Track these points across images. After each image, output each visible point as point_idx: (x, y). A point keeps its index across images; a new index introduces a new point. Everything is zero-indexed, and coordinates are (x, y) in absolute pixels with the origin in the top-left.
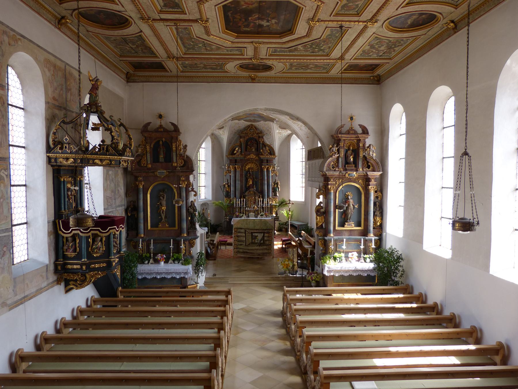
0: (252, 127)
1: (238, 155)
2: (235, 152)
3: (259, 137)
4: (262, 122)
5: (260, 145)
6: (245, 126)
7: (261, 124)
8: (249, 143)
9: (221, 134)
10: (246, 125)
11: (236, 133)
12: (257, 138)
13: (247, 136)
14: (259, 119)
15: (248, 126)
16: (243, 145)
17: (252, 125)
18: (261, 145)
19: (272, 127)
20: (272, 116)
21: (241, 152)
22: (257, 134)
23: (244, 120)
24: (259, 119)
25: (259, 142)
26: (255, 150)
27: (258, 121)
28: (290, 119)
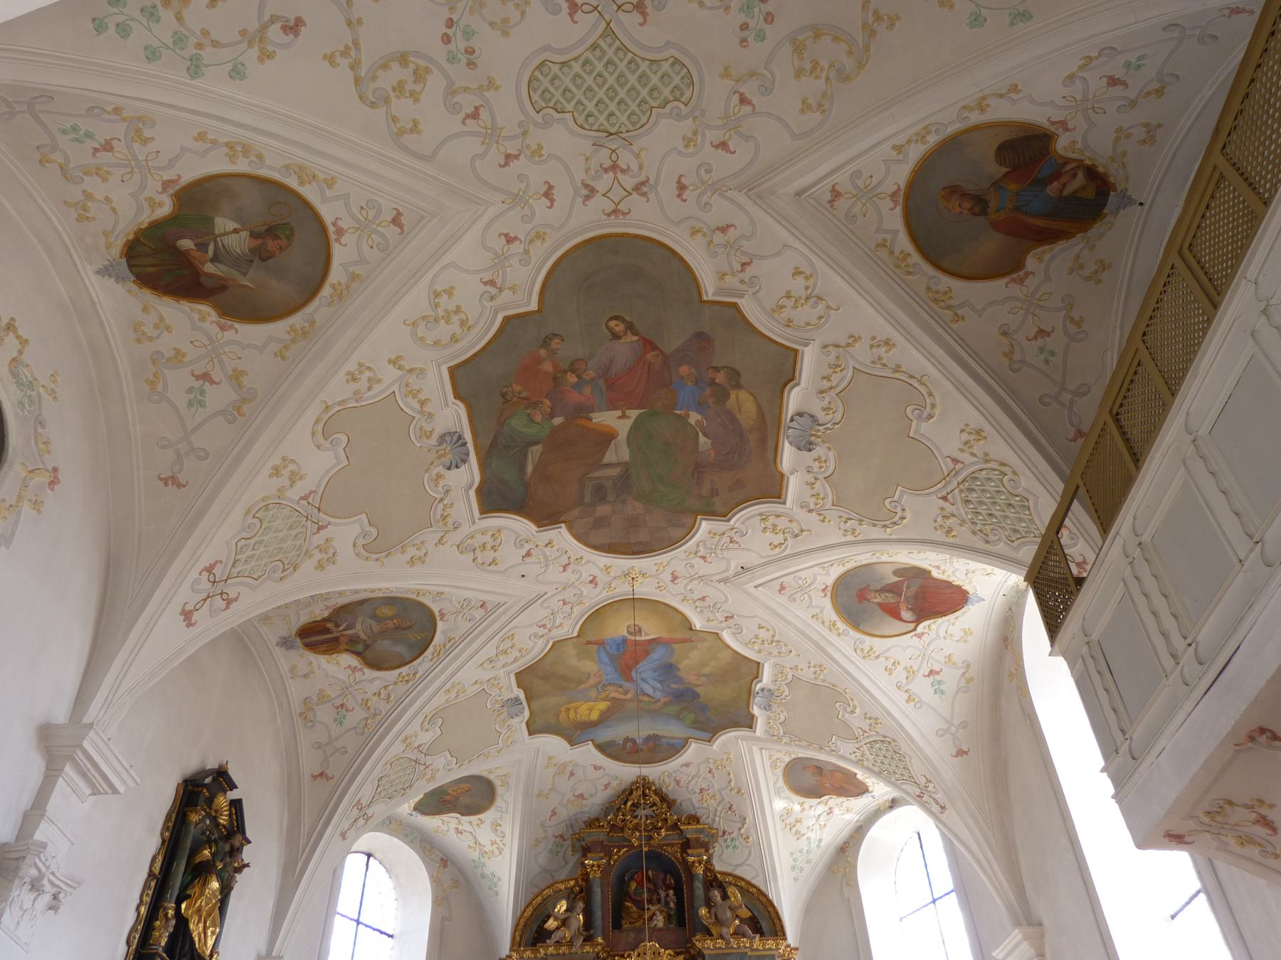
0: (645, 795)
1: (570, 944)
2: (551, 924)
3: (686, 845)
4: (693, 750)
5: (691, 889)
6: (610, 792)
7: (692, 770)
8: (633, 885)
9: (488, 848)
10: (616, 787)
11: (562, 836)
12: (673, 852)
13: (620, 848)
14: (671, 730)
15: (629, 792)
16: (597, 891)
17: (644, 785)
18: (699, 886)
19: (752, 785)
20: (737, 631)
21: (588, 924)
22: (675, 826)
23: (603, 748)
24: (671, 730)
25: (688, 868)
26: (668, 918)
27: (675, 749)
28: (841, 626)
